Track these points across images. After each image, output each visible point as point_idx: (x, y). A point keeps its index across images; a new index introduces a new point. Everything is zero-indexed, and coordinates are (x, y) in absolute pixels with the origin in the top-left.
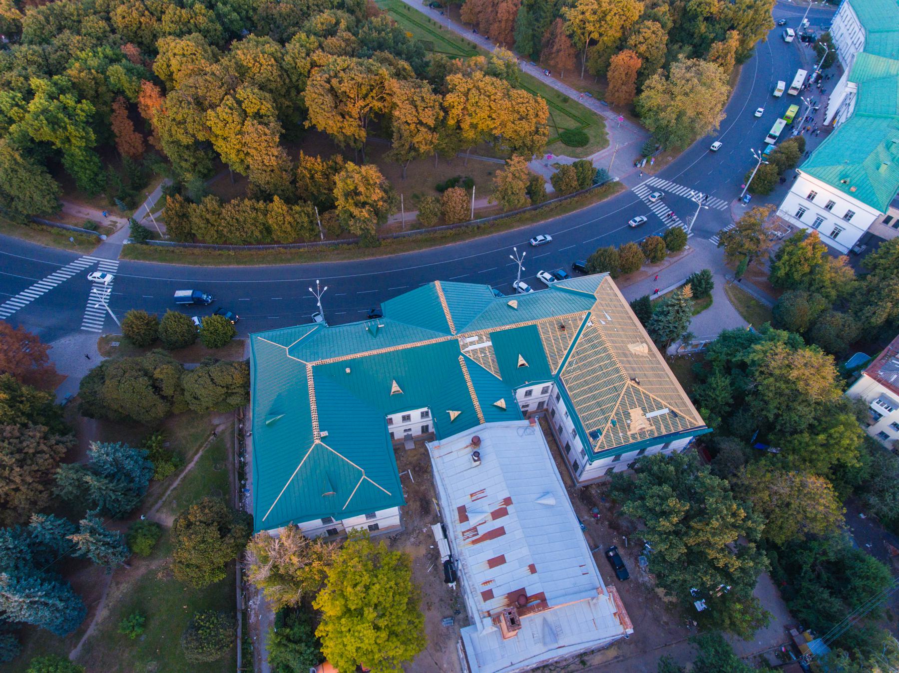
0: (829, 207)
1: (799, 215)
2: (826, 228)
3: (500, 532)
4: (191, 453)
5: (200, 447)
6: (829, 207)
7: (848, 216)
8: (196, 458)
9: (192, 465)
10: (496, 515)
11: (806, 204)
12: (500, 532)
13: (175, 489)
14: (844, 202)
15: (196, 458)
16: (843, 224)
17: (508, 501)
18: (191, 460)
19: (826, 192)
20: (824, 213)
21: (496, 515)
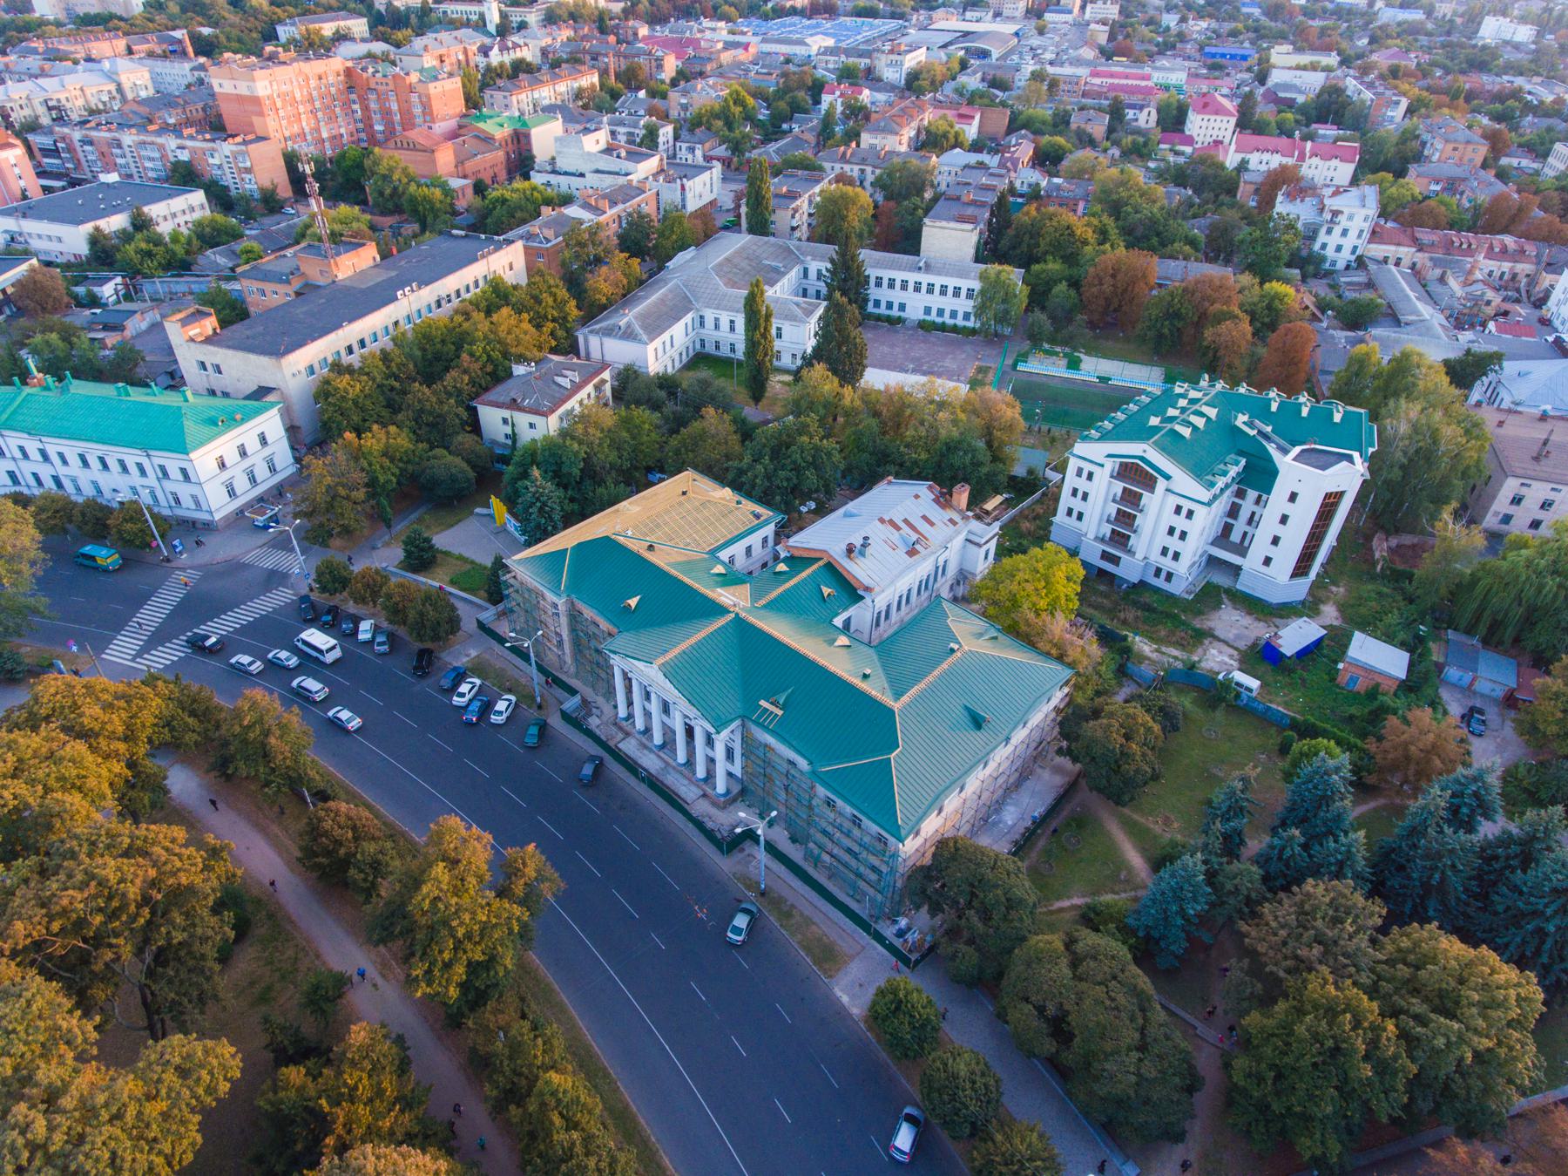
0: (243, 453)
1: (232, 493)
2: (262, 472)
3: (906, 521)
4: (1067, 916)
5: (1052, 913)
6: (243, 453)
7: (263, 441)
8: (1066, 903)
9: (1076, 901)
10: (898, 528)
11: (226, 475)
12: (906, 521)
13: (1114, 892)
14: (247, 434)
15: (1066, 903)
16: (267, 451)
17: (882, 521)
18: (1074, 907)
19: (225, 445)
20: (247, 463)
21: (898, 528)
